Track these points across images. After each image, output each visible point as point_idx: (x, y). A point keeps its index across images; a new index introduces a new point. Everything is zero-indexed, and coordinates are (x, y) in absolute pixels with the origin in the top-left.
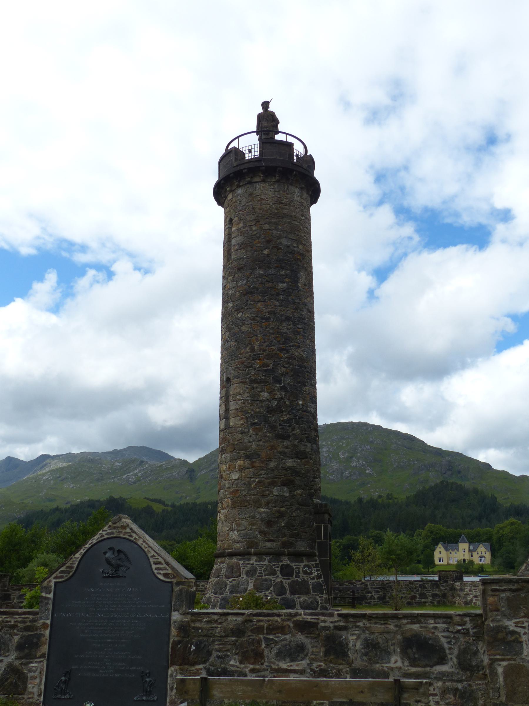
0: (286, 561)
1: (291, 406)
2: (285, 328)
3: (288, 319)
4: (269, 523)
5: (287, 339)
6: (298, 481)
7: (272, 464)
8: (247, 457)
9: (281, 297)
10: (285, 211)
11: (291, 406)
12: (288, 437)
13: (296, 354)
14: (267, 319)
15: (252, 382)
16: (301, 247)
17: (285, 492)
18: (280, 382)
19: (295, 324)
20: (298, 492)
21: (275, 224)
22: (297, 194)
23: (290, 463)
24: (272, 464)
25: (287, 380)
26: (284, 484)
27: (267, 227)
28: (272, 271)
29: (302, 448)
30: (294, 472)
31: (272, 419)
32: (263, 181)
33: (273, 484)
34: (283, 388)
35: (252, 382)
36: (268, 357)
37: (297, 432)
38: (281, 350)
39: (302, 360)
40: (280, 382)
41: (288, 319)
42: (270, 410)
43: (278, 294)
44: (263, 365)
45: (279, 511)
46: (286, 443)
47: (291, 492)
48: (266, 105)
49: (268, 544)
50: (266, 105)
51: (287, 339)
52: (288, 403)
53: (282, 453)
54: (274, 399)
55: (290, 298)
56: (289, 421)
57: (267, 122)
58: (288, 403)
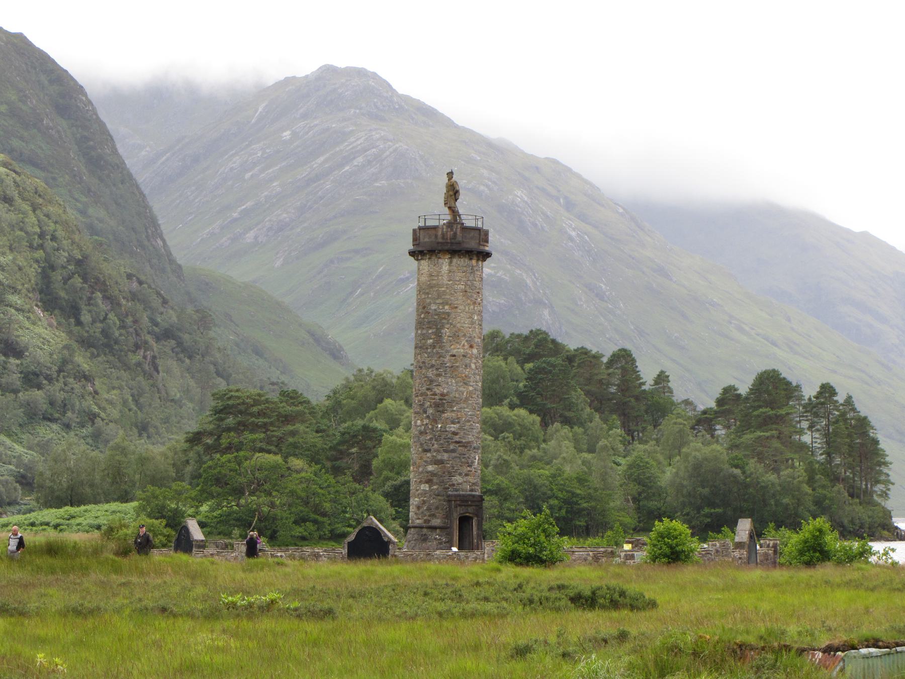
0: (425, 531)
1: (432, 429)
2: (431, 373)
3: (433, 366)
6: (435, 480)
7: (421, 469)
10: (434, 282)
12: (429, 451)
13: (438, 392)
14: (421, 368)
16: (447, 307)
19: (437, 369)
21: (428, 294)
23: (430, 468)
24: (421, 469)
25: (430, 411)
26: (427, 482)
27: (423, 296)
28: (424, 331)
29: (439, 457)
30: (433, 474)
31: (422, 438)
34: (428, 417)
36: (422, 395)
37: (436, 446)
38: (428, 389)
39: (442, 395)
40: (425, 412)
42: (421, 433)
44: (419, 401)
45: (424, 501)
46: (429, 455)
48: (450, 174)
49: (418, 521)
50: (450, 174)
51: (431, 381)
53: (425, 462)
56: (431, 439)
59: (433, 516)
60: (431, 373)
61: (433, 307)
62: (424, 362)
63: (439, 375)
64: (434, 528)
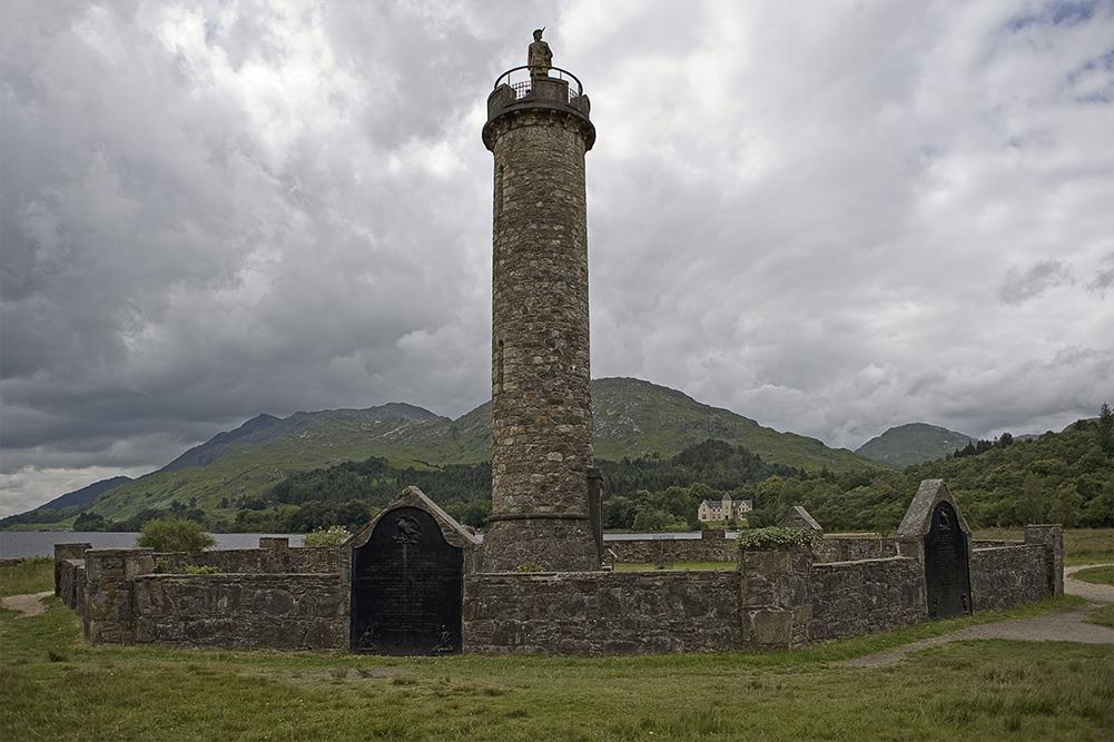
2: (559, 287)
3: (561, 279)
4: (543, 488)
5: (561, 300)
6: (571, 446)
7: (546, 430)
8: (521, 423)
9: (554, 255)
11: (564, 370)
15: (525, 345)
17: (559, 457)
18: (553, 346)
20: (573, 457)
22: (570, 137)
23: (563, 428)
24: (546, 430)
29: (575, 413)
31: (546, 384)
32: (536, 124)
33: (547, 450)
34: (556, 352)
35: (525, 345)
36: (542, 318)
38: (554, 312)
40: (553, 346)
41: (561, 279)
42: (544, 375)
43: (552, 252)
45: (553, 476)
46: (560, 408)
47: (564, 458)
48: (538, 34)
49: (542, 509)
50: (538, 34)
52: (561, 367)
54: (549, 363)
55: (563, 256)
57: (540, 54)
58: (561, 367)
59: (570, 500)
60: (559, 287)
61: (559, 194)
62: (546, 272)
63: (569, 294)
64: (573, 519)
